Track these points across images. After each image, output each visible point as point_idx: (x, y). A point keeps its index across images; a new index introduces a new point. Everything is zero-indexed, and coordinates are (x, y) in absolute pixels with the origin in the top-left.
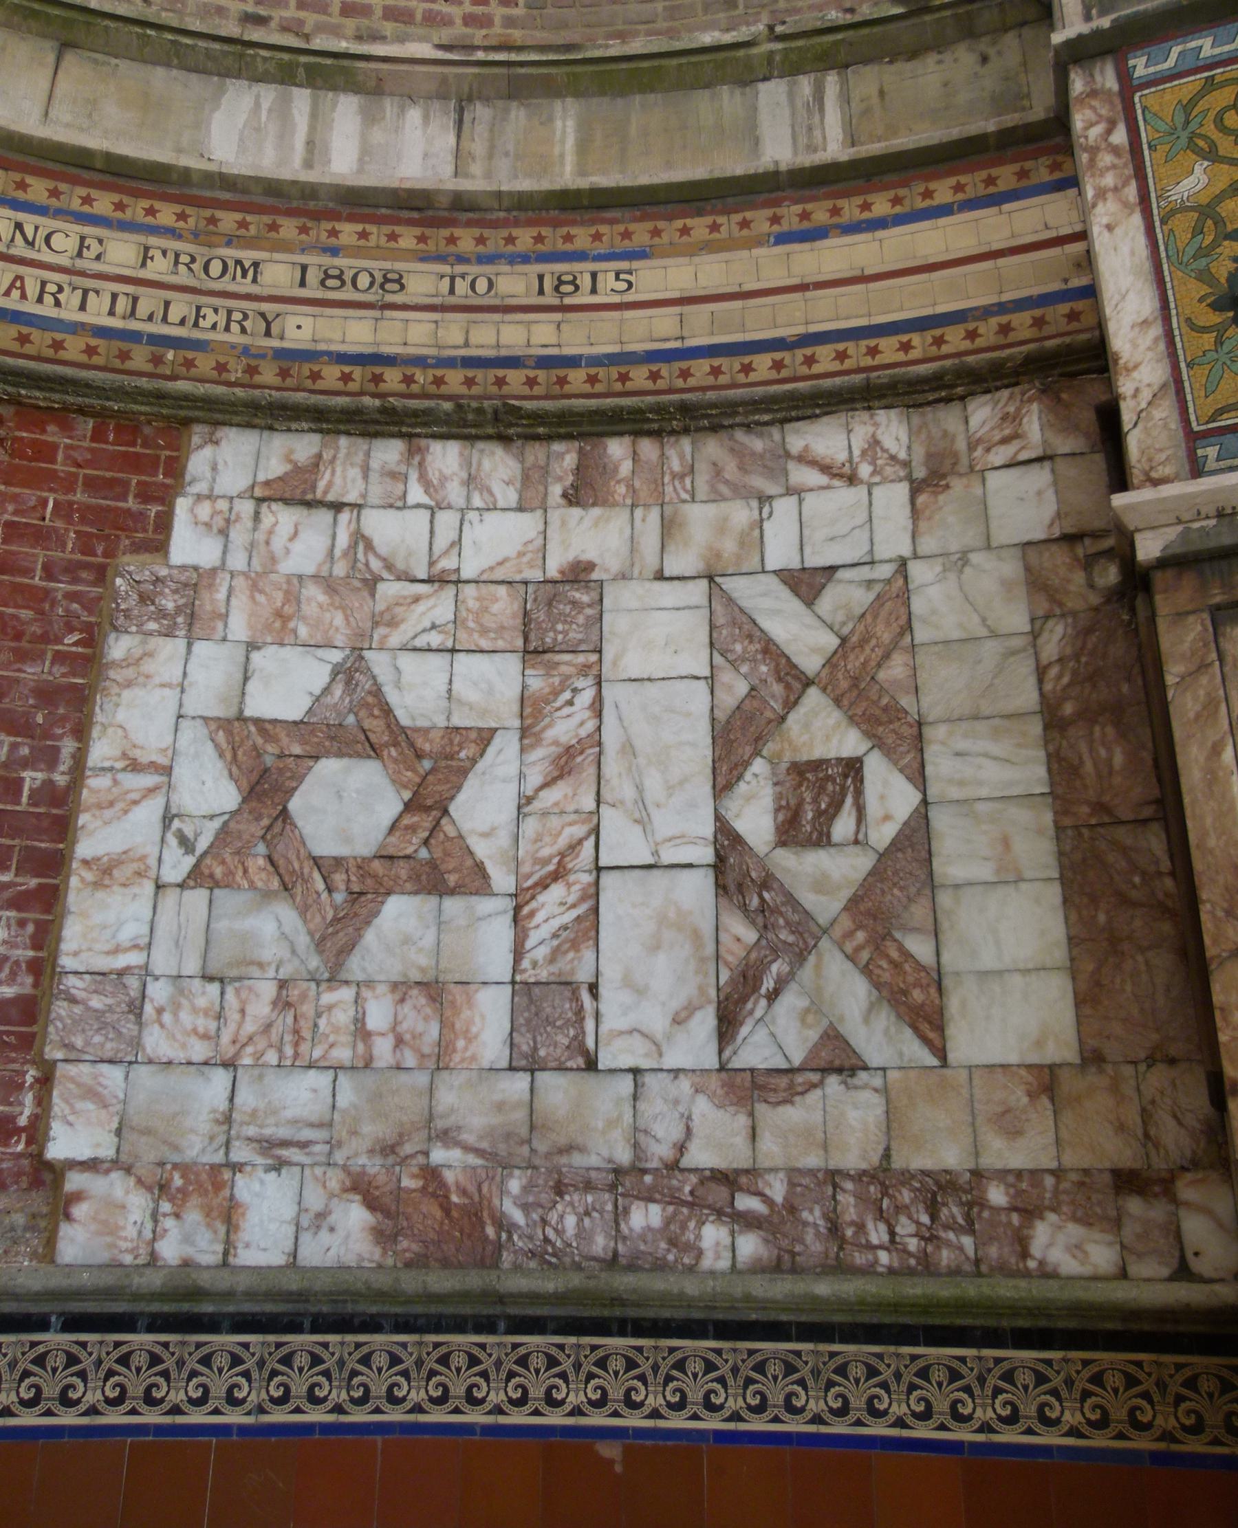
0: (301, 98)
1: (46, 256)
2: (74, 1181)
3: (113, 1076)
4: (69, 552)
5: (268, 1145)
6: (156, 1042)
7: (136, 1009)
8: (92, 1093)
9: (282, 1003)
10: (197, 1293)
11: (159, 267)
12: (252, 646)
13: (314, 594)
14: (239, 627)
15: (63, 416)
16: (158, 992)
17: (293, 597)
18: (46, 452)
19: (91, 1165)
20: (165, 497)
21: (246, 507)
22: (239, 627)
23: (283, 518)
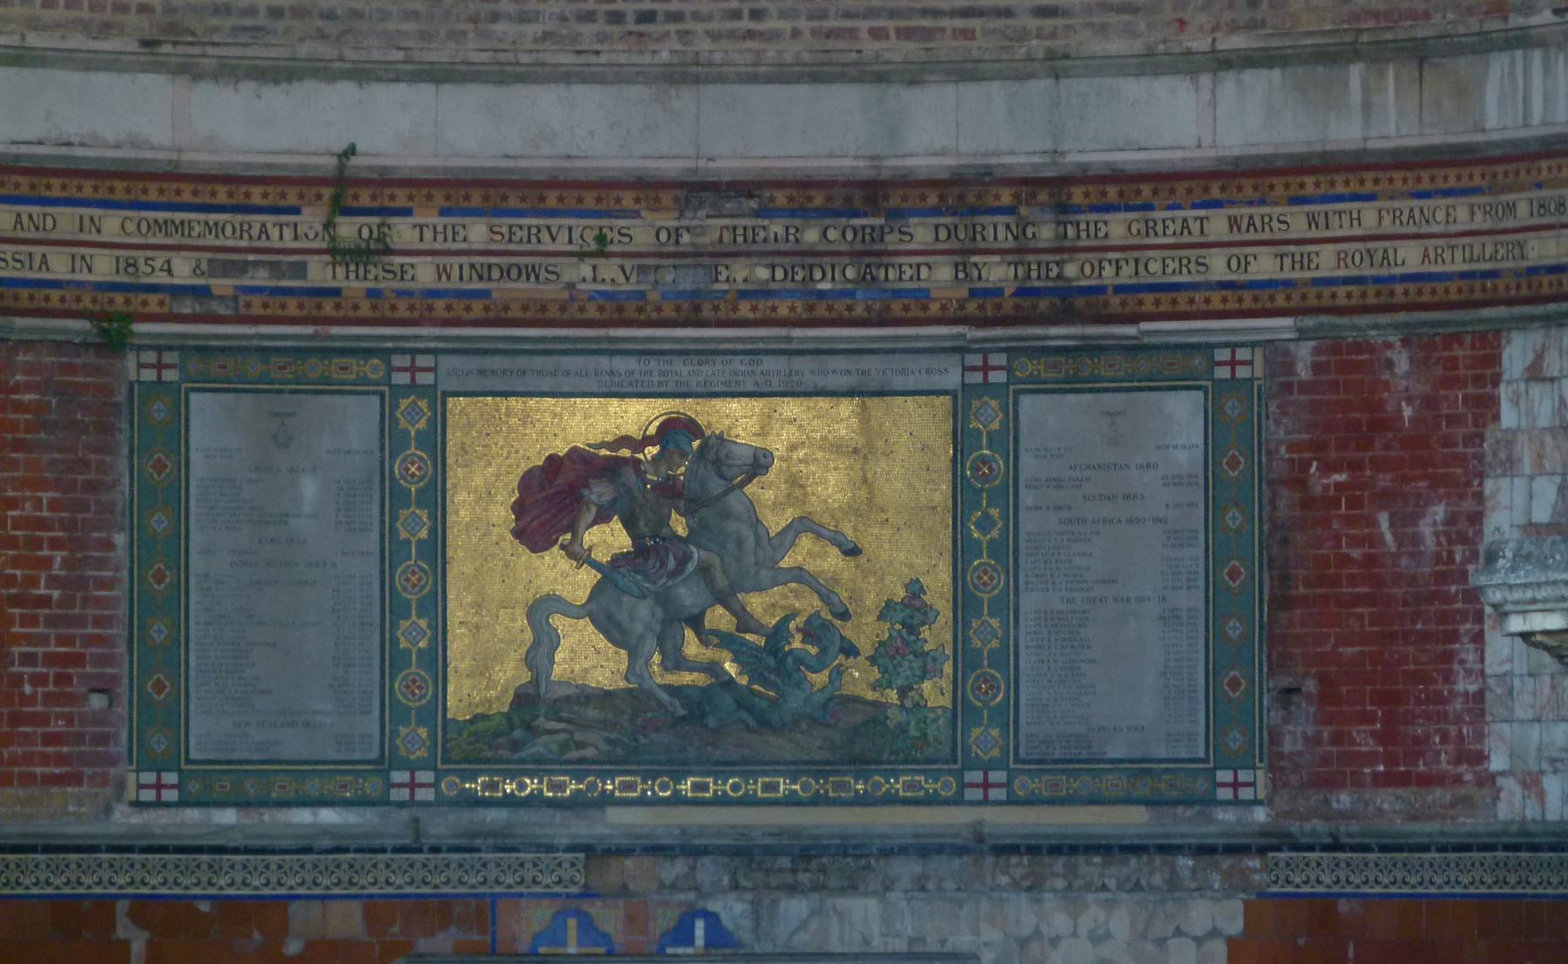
0: (1519, 54)
1: (1435, 229)
2: (1500, 781)
3: (1506, 727)
4: (1470, 429)
5: (1553, 761)
6: (1520, 712)
7: (1510, 691)
8: (1502, 738)
9: (1553, 688)
10: (1528, 834)
11: (1480, 222)
12: (1532, 478)
13: (1548, 439)
14: (1527, 468)
15: (1456, 338)
16: (1517, 683)
17: (1542, 444)
18: (1453, 363)
19: (1503, 774)
20: (1496, 383)
21: (1522, 386)
22: (1527, 468)
23: (1536, 389)
